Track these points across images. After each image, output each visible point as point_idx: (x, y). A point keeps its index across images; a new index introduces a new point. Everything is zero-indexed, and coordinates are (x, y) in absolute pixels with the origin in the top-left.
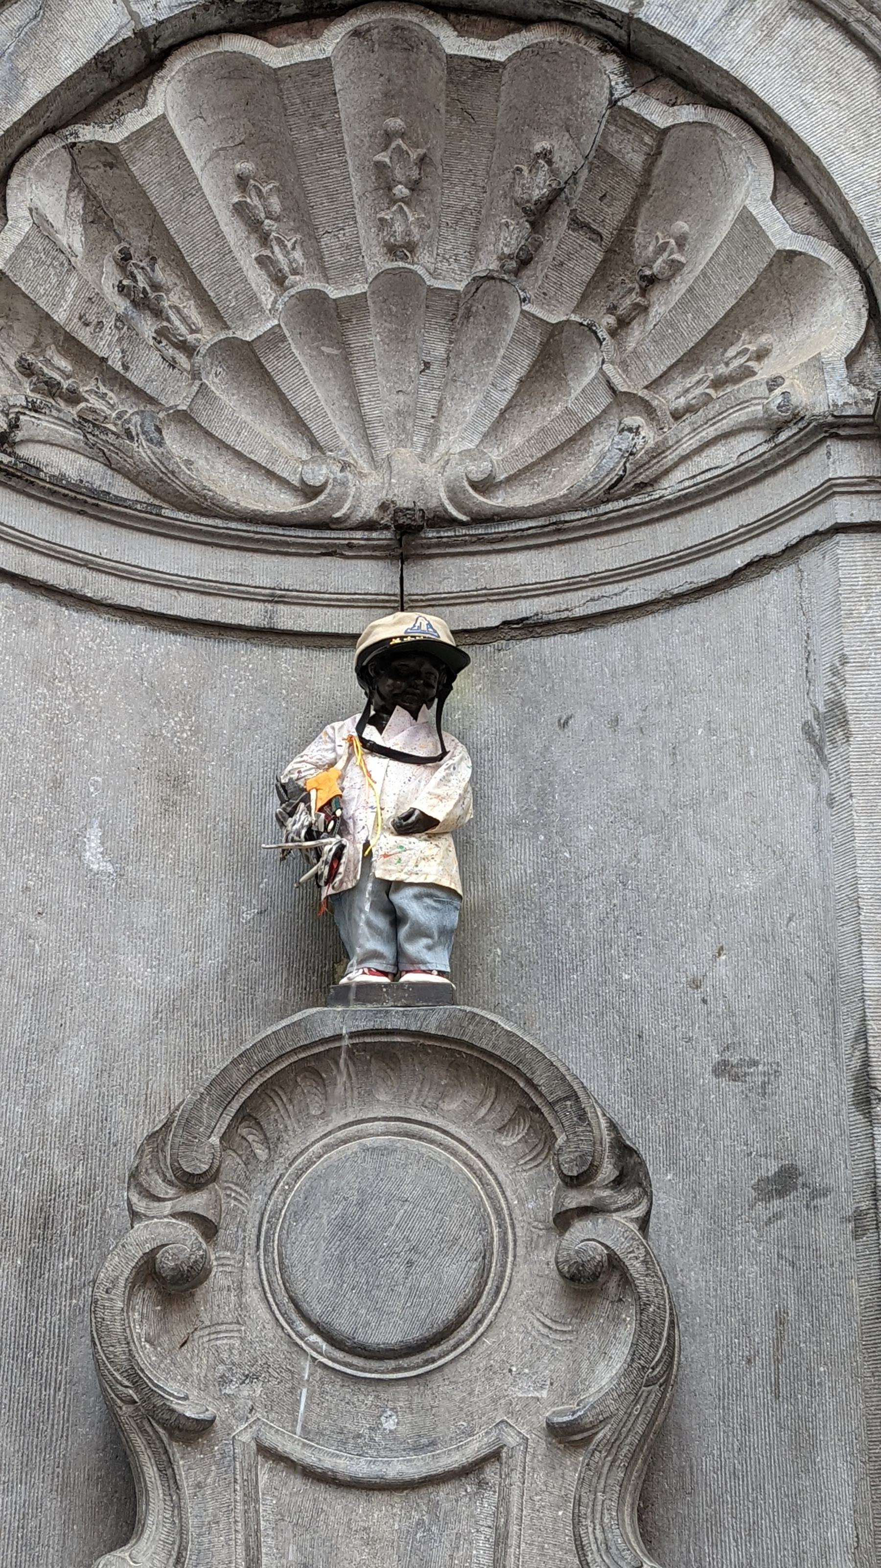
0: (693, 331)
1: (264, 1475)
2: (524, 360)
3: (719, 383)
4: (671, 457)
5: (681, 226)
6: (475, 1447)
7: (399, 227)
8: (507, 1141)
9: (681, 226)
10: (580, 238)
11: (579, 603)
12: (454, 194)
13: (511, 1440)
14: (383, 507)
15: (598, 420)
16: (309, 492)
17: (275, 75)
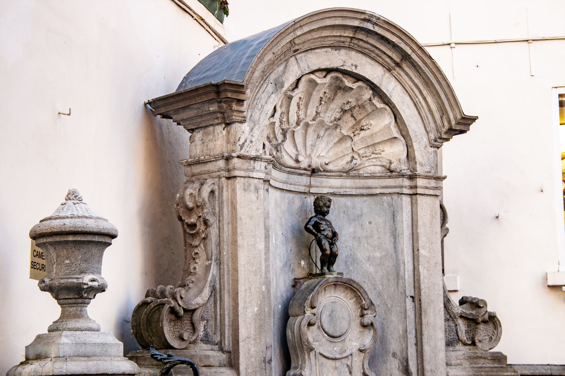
0: (370, 142)
1: (321, 358)
2: (336, 140)
3: (373, 153)
4: (362, 166)
5: (372, 122)
6: (348, 353)
7: (320, 109)
8: (351, 301)
9: (372, 122)
10: (352, 119)
11: (342, 191)
12: (333, 106)
13: (354, 351)
14: (310, 166)
15: (348, 154)
16: (297, 161)
17: (316, 84)
